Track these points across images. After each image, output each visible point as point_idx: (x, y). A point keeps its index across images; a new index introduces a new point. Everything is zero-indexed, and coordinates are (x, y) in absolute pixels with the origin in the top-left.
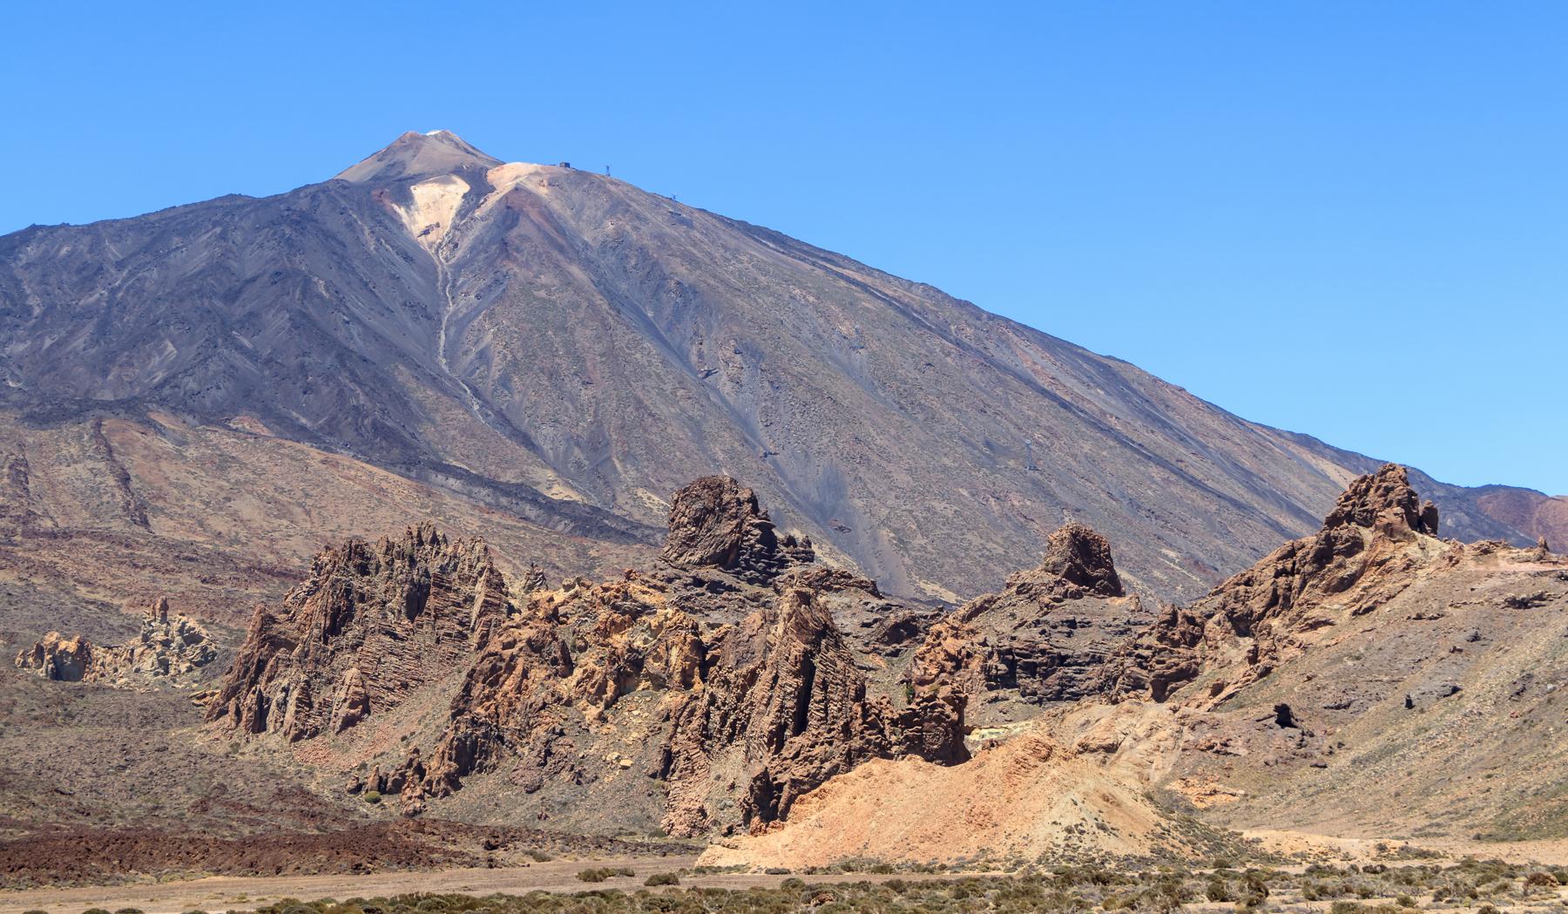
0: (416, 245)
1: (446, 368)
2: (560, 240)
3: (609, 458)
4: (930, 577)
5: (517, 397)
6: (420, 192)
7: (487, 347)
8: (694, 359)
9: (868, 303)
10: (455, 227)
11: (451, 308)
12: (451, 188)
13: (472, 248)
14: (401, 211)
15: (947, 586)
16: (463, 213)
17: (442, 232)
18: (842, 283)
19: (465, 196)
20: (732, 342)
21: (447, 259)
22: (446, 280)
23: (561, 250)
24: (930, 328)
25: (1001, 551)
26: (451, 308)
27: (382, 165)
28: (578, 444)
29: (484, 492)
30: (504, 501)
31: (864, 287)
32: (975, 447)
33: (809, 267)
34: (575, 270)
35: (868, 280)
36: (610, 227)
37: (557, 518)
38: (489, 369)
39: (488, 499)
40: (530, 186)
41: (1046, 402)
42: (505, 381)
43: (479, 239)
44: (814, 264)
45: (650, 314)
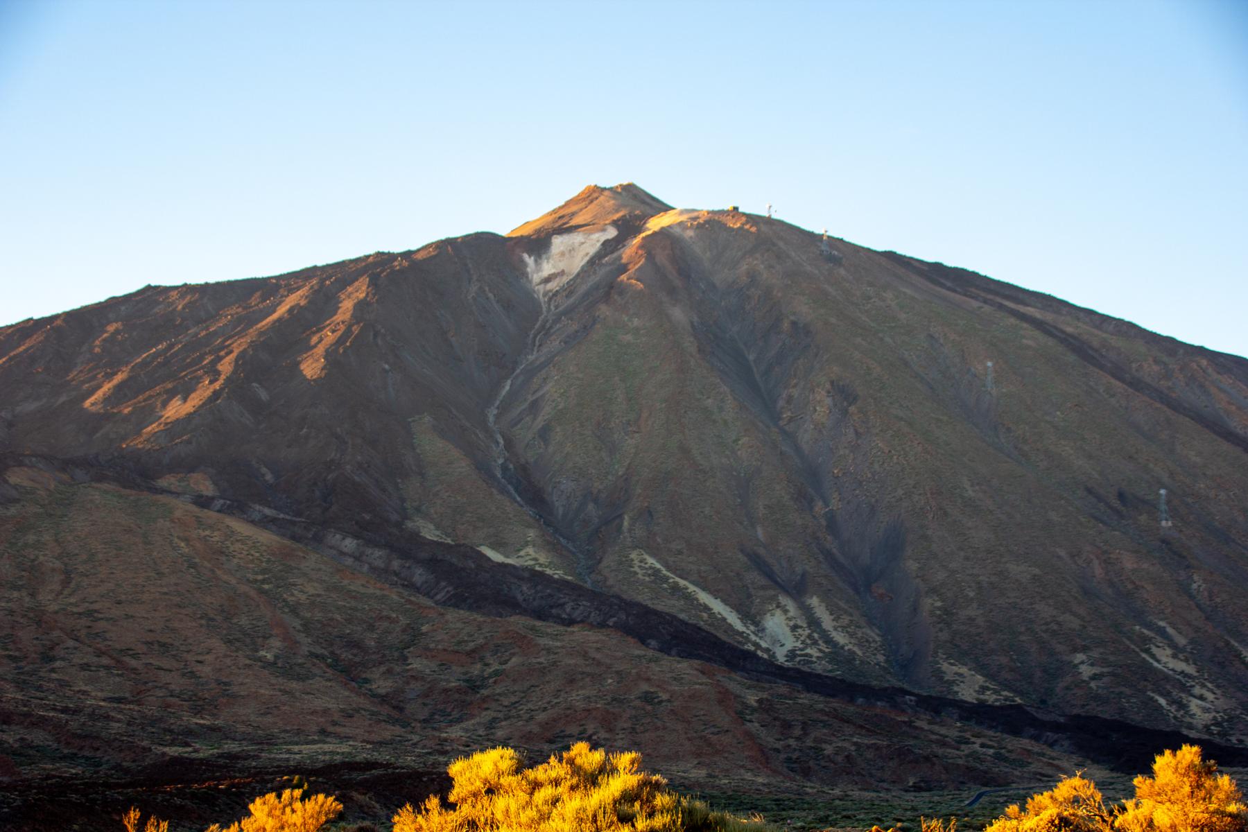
0: (529, 295)
1: (491, 419)
2: (678, 282)
3: (620, 516)
4: (960, 656)
5: (551, 449)
6: (558, 243)
7: (543, 396)
8: (781, 403)
9: (1031, 338)
10: (578, 274)
11: (531, 358)
12: (596, 236)
13: (587, 294)
14: (530, 260)
15: (981, 668)
16: (594, 261)
17: (565, 279)
18: (1013, 320)
19: (606, 243)
20: (828, 386)
21: (557, 307)
22: (543, 327)
23: (672, 291)
24: (1102, 367)
25: (1075, 623)
26: (531, 358)
27: (550, 218)
28: (596, 501)
29: (378, 553)
30: (396, 564)
31: (1039, 325)
32: (1099, 498)
33: (975, 304)
34: (678, 314)
35: (1049, 317)
36: (744, 267)
37: (443, 584)
38: (535, 419)
39: (379, 564)
40: (678, 230)
41: (1225, 446)
42: (544, 434)
43: (596, 287)
44: (985, 301)
45: (751, 357)
